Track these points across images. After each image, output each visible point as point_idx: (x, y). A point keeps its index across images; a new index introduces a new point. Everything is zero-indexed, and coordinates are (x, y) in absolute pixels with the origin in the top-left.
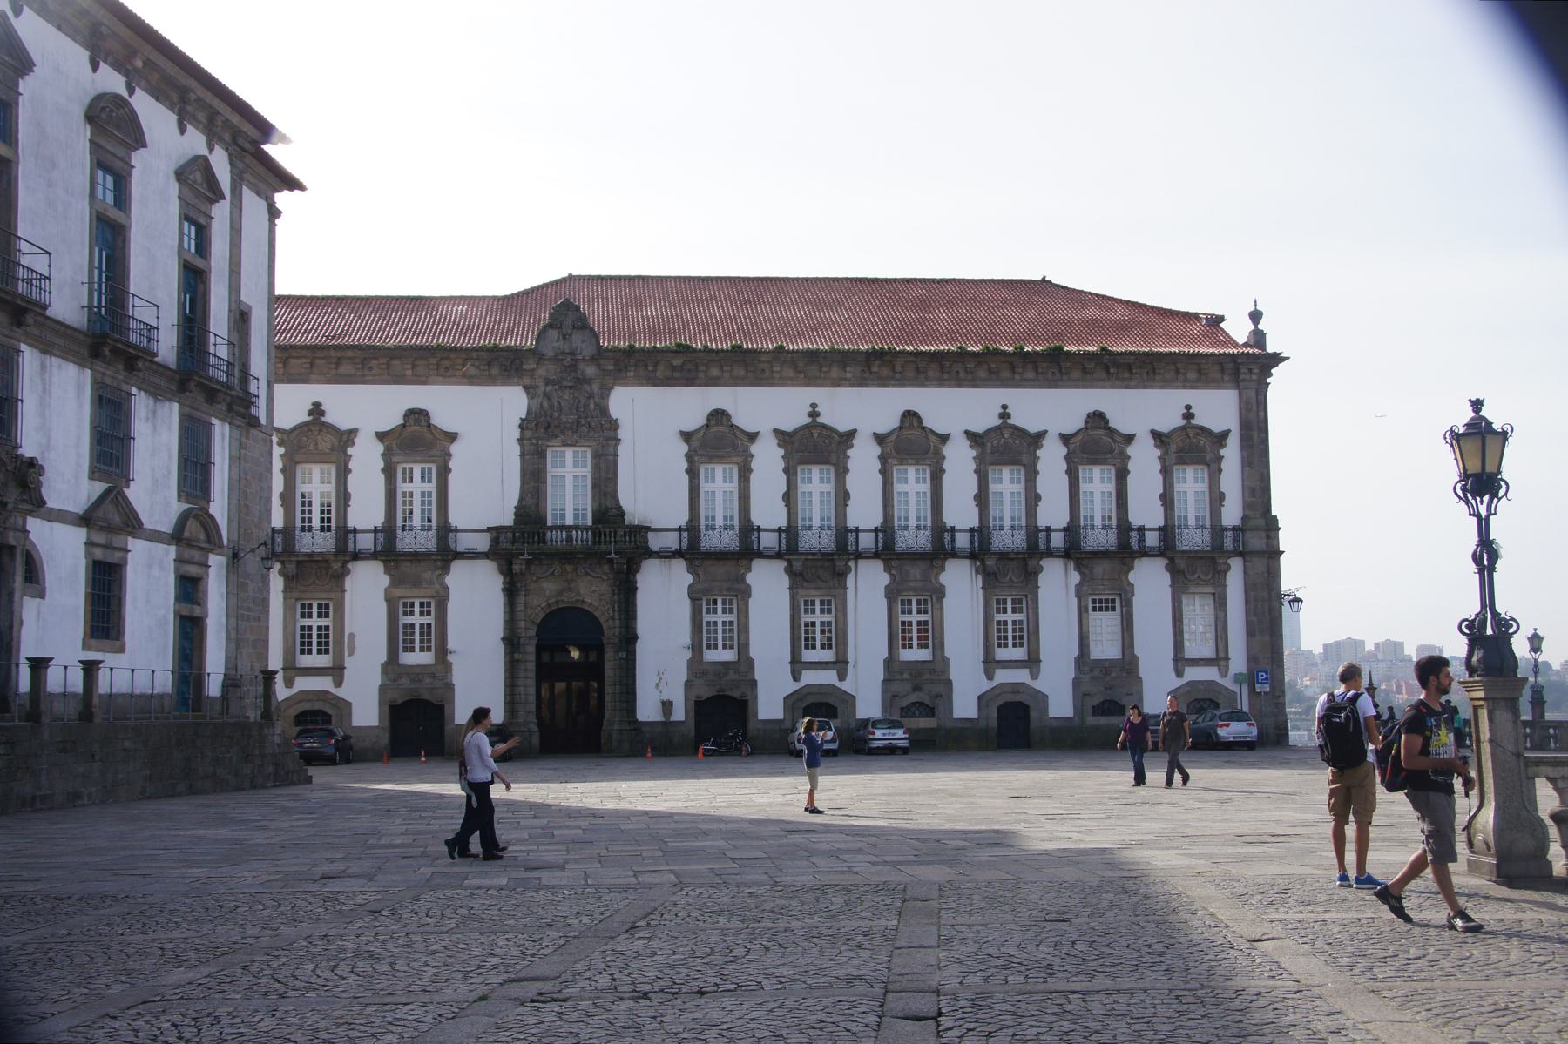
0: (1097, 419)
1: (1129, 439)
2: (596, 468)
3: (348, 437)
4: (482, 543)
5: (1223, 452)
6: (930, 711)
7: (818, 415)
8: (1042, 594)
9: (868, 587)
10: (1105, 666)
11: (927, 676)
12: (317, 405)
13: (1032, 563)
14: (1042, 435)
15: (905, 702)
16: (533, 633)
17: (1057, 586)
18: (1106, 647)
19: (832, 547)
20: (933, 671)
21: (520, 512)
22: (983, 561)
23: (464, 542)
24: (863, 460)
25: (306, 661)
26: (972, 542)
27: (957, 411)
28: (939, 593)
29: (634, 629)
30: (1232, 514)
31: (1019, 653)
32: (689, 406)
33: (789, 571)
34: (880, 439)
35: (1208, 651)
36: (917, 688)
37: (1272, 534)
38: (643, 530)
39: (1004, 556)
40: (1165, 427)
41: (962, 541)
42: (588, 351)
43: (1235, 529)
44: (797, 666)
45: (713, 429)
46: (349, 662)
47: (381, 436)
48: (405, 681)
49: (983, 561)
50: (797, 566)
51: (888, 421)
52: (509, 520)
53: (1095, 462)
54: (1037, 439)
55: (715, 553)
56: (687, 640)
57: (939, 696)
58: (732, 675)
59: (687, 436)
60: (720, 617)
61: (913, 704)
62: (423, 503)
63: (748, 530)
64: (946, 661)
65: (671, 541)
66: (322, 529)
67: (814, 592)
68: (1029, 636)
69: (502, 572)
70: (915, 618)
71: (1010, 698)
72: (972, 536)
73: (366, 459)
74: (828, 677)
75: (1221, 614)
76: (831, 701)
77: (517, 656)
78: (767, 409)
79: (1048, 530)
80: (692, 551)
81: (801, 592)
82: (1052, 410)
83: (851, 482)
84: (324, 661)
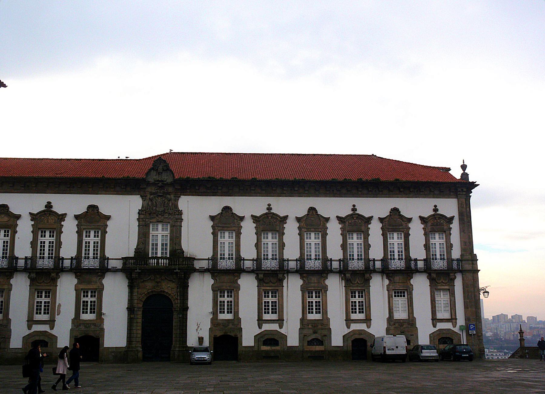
0: (395, 211)
1: (410, 220)
2: (171, 231)
3: (63, 217)
4: (119, 265)
5: (451, 226)
6: (321, 343)
7: (271, 209)
9: (293, 287)
11: (320, 326)
12: (49, 203)
13: (367, 276)
14: (371, 218)
15: (310, 339)
16: (141, 306)
17: (378, 287)
19: (277, 268)
20: (322, 324)
21: (137, 251)
22: (345, 275)
23: (112, 264)
24: (291, 230)
25: (37, 317)
26: (340, 266)
27: (334, 207)
28: (326, 288)
29: (187, 304)
30: (456, 254)
31: (362, 316)
32: (214, 205)
33: (257, 278)
34: (298, 219)
35: (447, 316)
36: (315, 332)
37: (474, 262)
38: (192, 259)
39: (355, 273)
40: (426, 215)
41: (335, 265)
42: (170, 180)
43: (458, 260)
44: (260, 322)
46: (57, 318)
47: (77, 217)
48: (82, 327)
49: (345, 275)
50: (261, 276)
51: (302, 212)
52: (132, 255)
55: (224, 270)
56: (211, 310)
58: (231, 326)
59: (212, 218)
60: (226, 299)
61: (313, 339)
62: (94, 247)
63: (239, 259)
64: (328, 320)
65: (204, 265)
66: (49, 258)
67: (268, 288)
69: (127, 278)
70: (314, 300)
71: (357, 337)
72: (340, 263)
73: (70, 228)
74: (275, 327)
75: (453, 299)
76: (276, 337)
77: (132, 316)
78: (248, 207)
79: (374, 260)
80: (214, 271)
81: (263, 288)
82: (375, 207)
83: (286, 239)
84: (46, 317)
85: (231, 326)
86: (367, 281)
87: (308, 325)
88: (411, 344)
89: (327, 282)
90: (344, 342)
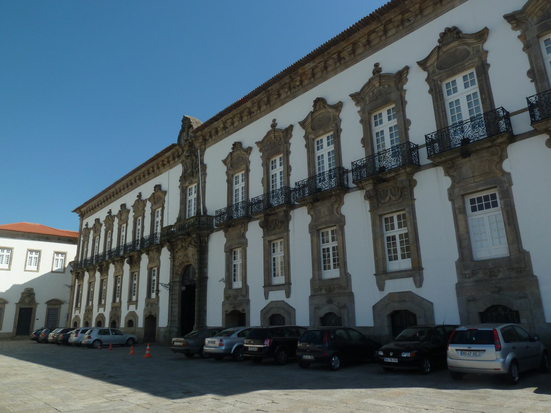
1: (482, 35)
8: (418, 205)
10: (491, 268)
18: (491, 244)
21: (179, 219)
28: (341, 222)
29: (206, 273)
31: (406, 264)
36: (330, 302)
45: (235, 154)
53: (455, 73)
54: (401, 76)
57: (345, 307)
58: (240, 298)
59: (225, 162)
68: (412, 246)
71: (397, 307)
85: (240, 298)
86: (406, 193)
87: (321, 290)
88: (523, 321)
89: (344, 210)
90: (374, 318)
